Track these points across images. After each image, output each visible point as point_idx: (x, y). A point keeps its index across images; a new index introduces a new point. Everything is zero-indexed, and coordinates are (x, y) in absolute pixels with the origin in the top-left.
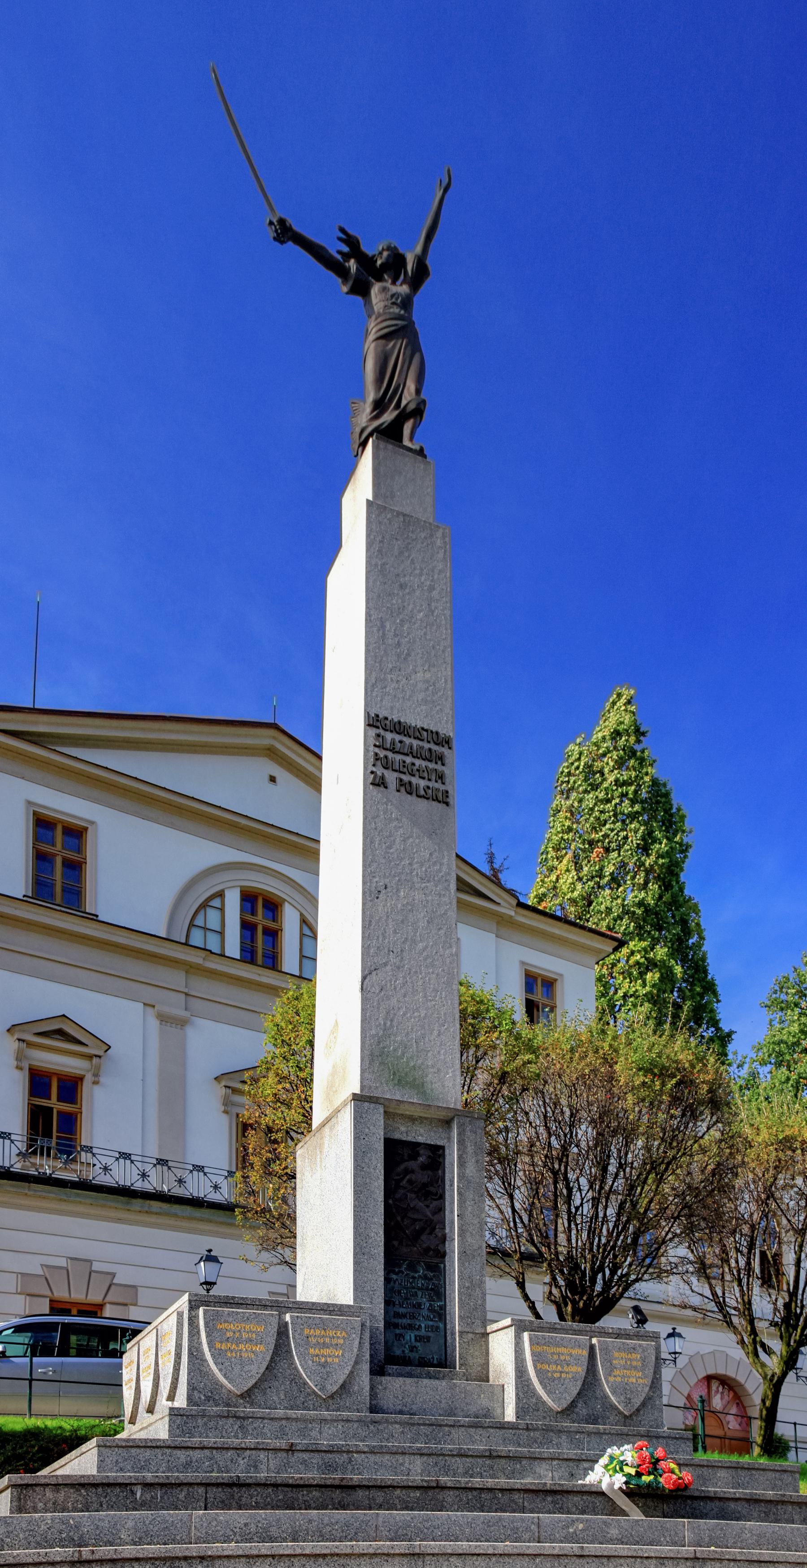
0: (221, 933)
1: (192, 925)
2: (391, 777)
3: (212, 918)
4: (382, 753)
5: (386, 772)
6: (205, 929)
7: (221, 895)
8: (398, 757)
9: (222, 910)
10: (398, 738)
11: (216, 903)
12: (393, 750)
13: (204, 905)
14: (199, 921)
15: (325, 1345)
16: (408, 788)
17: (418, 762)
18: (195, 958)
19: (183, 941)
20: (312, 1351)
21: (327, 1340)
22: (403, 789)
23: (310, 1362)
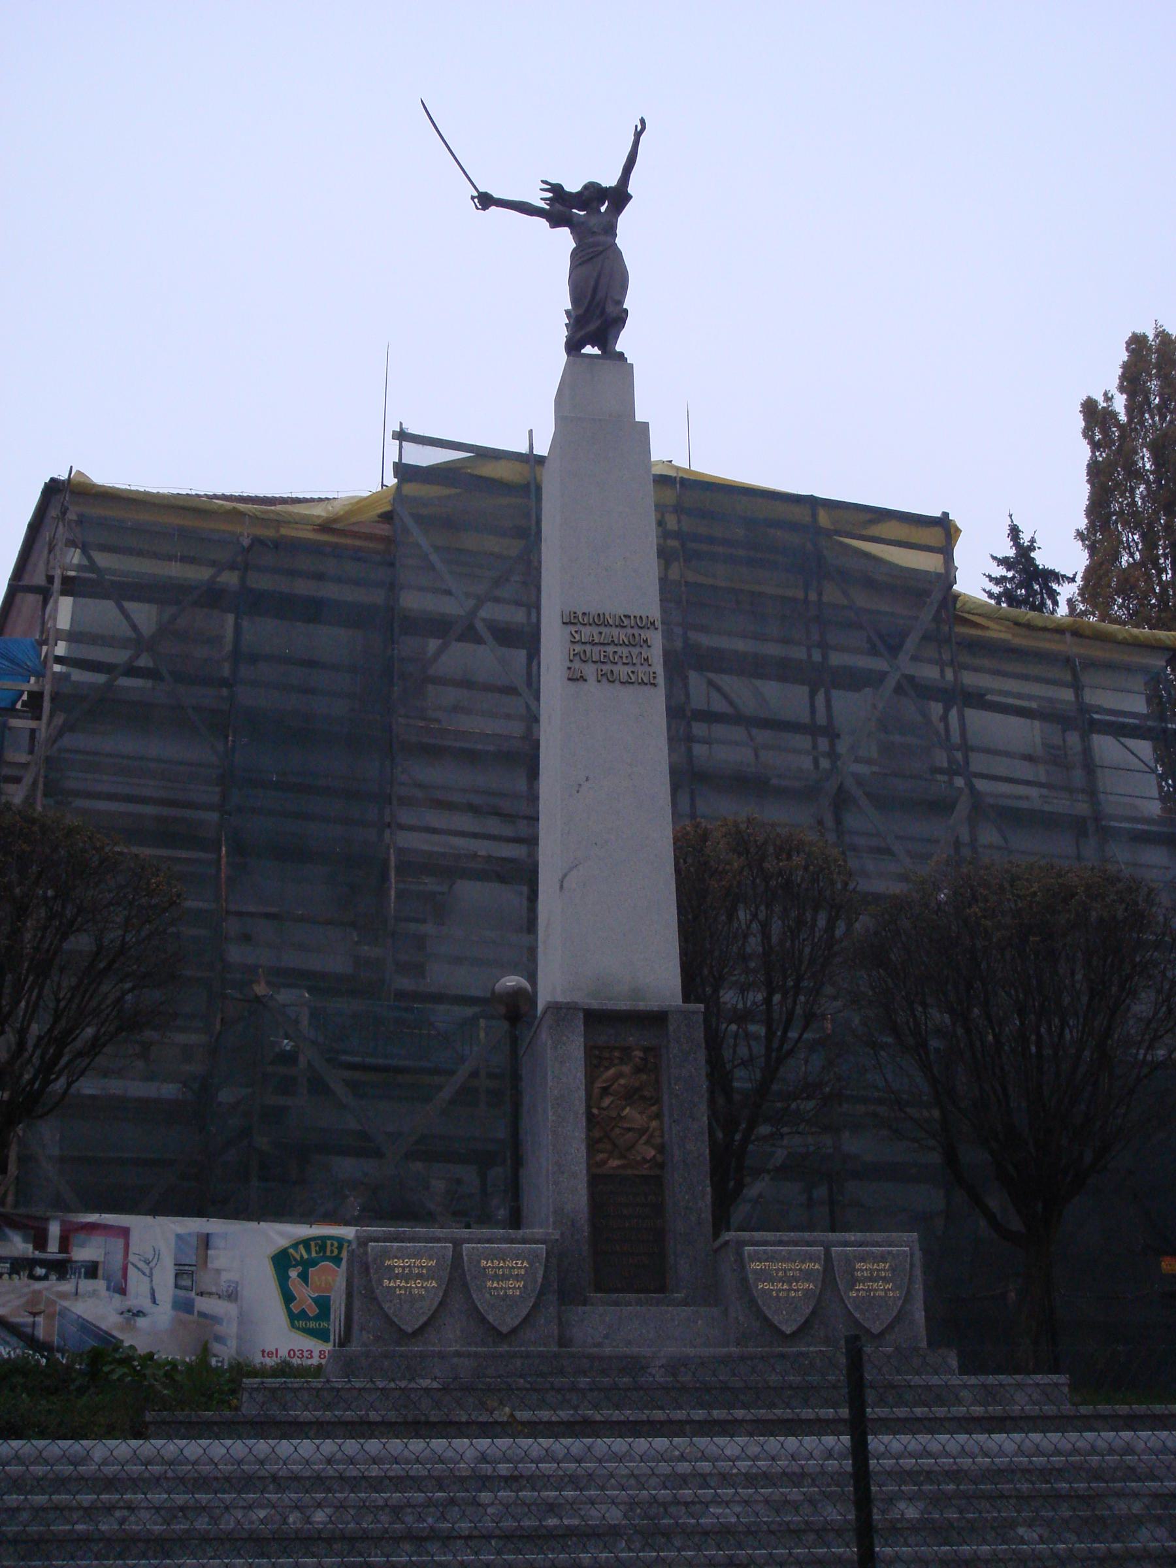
2: (590, 670)
4: (578, 648)
15: (505, 1278)
16: (609, 678)
20: (489, 1284)
21: (507, 1272)
22: (604, 680)
23: (487, 1296)
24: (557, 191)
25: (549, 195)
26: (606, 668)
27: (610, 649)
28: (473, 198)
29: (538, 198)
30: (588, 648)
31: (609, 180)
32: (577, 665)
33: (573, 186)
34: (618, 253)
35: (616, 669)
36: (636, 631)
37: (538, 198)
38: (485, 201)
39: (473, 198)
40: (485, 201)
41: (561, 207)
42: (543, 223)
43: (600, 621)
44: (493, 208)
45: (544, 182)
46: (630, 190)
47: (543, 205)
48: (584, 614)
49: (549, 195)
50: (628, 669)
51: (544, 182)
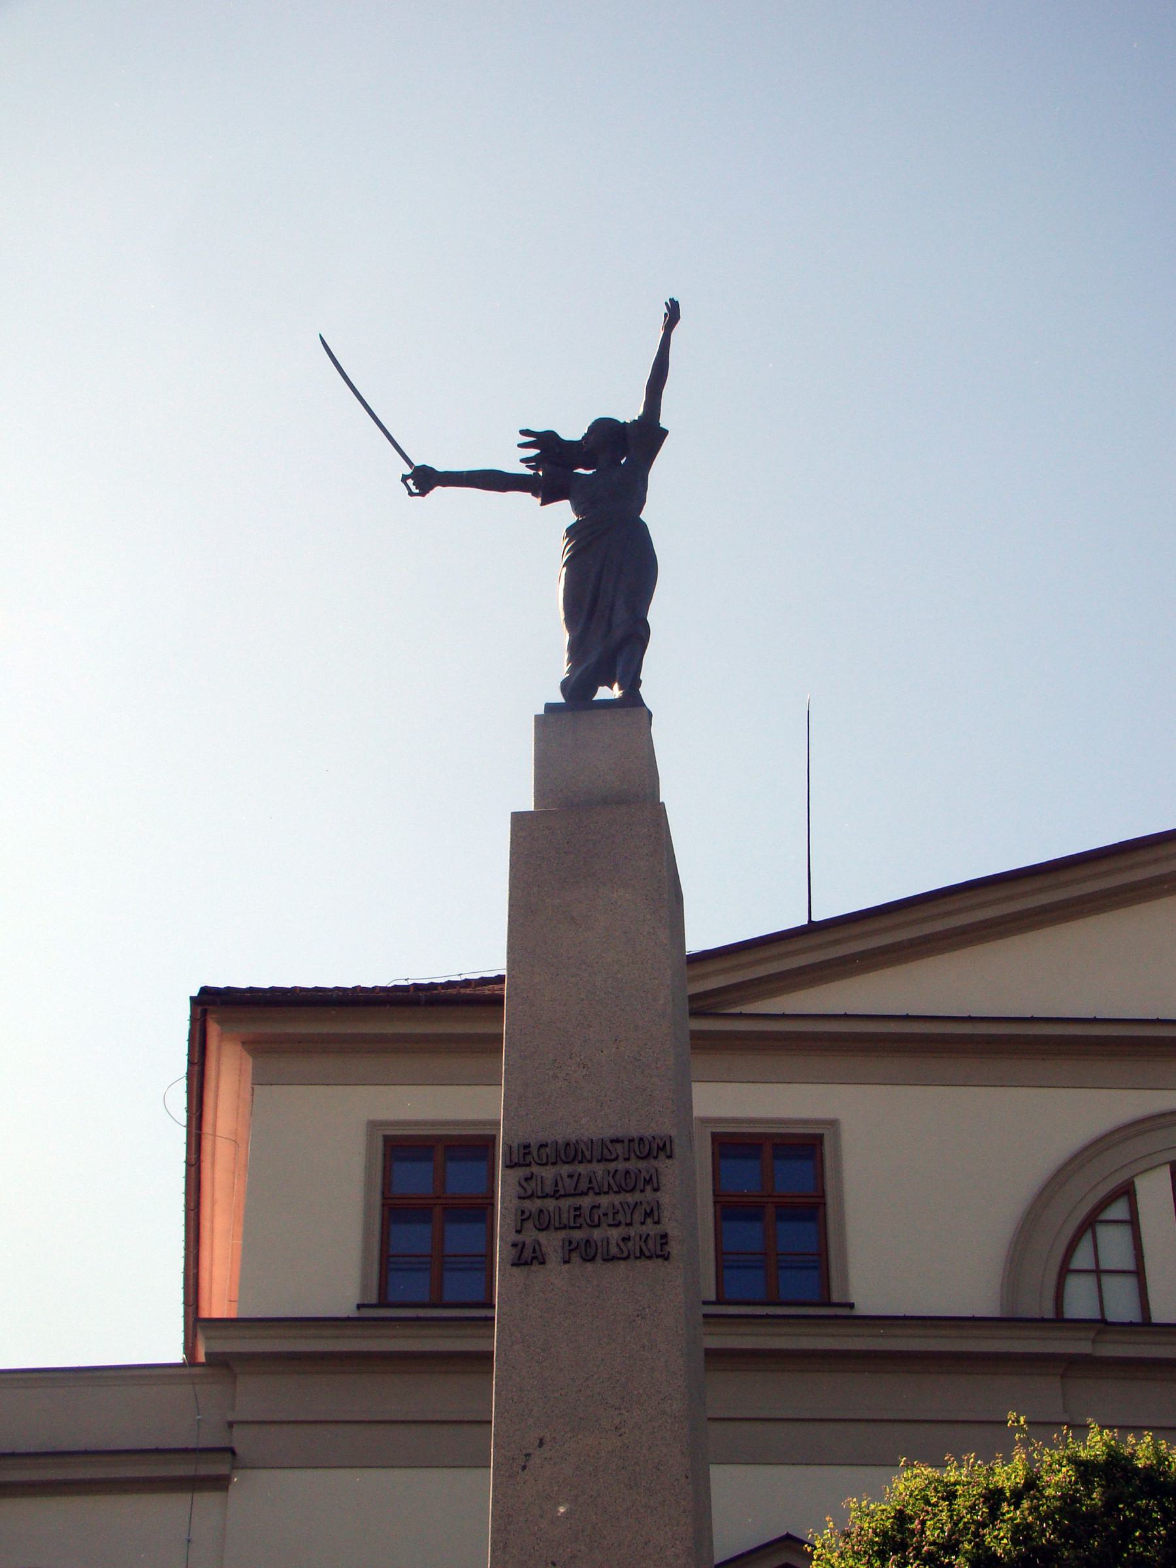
0: (1139, 1273)
1: (1065, 1270)
2: (551, 1242)
3: (1113, 1245)
5: (542, 1237)
6: (1098, 1272)
7: (1127, 1191)
8: (565, 1203)
9: (1133, 1222)
10: (565, 1169)
11: (1118, 1210)
12: (556, 1195)
13: (1090, 1223)
14: (1082, 1258)
16: (588, 1252)
17: (604, 1200)
18: (1082, 1346)
19: (1049, 1313)
22: (575, 1257)
24: (546, 445)
25: (533, 452)
26: (578, 1235)
27: (586, 1202)
28: (404, 479)
29: (512, 460)
30: (551, 1204)
31: (629, 410)
32: (530, 1235)
33: (573, 431)
34: (643, 527)
35: (597, 1234)
36: (634, 1165)
37: (512, 460)
38: (424, 480)
39: (404, 479)
40: (424, 480)
41: (554, 466)
42: (526, 500)
43: (570, 1152)
44: (438, 489)
45: (525, 433)
46: (663, 423)
47: (524, 470)
48: (543, 1146)
49: (533, 452)
50: (615, 1234)
51: (525, 433)
